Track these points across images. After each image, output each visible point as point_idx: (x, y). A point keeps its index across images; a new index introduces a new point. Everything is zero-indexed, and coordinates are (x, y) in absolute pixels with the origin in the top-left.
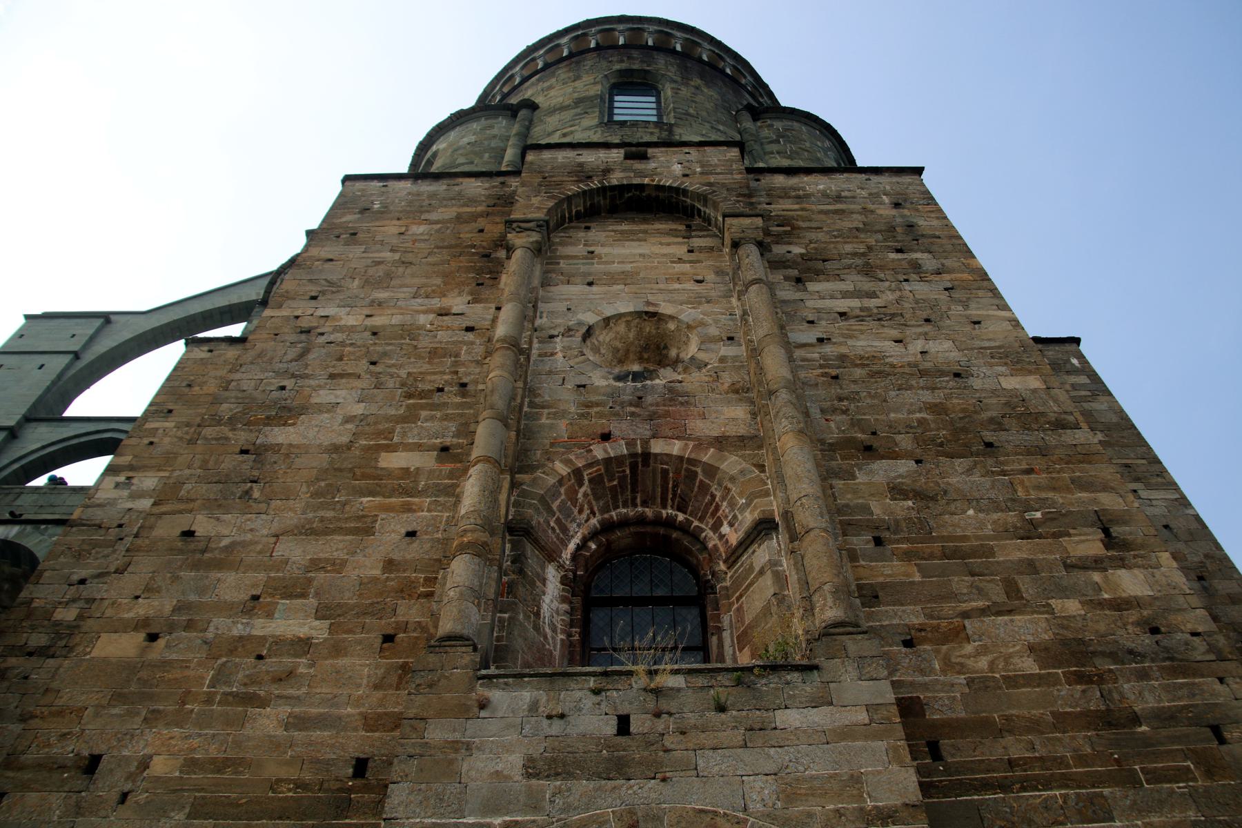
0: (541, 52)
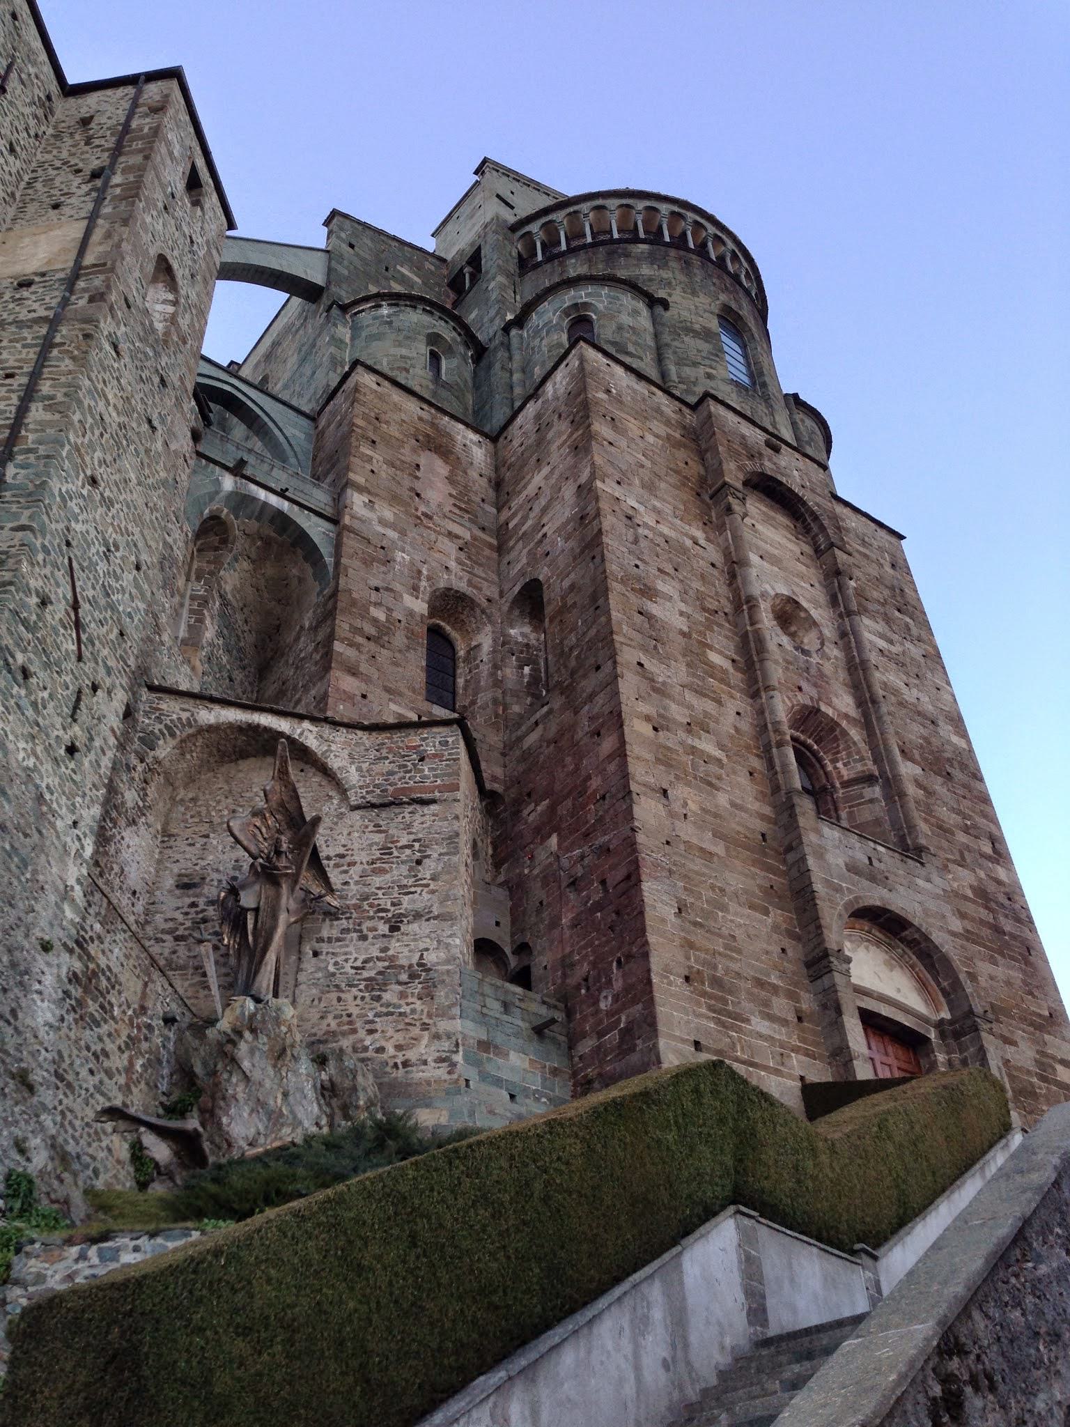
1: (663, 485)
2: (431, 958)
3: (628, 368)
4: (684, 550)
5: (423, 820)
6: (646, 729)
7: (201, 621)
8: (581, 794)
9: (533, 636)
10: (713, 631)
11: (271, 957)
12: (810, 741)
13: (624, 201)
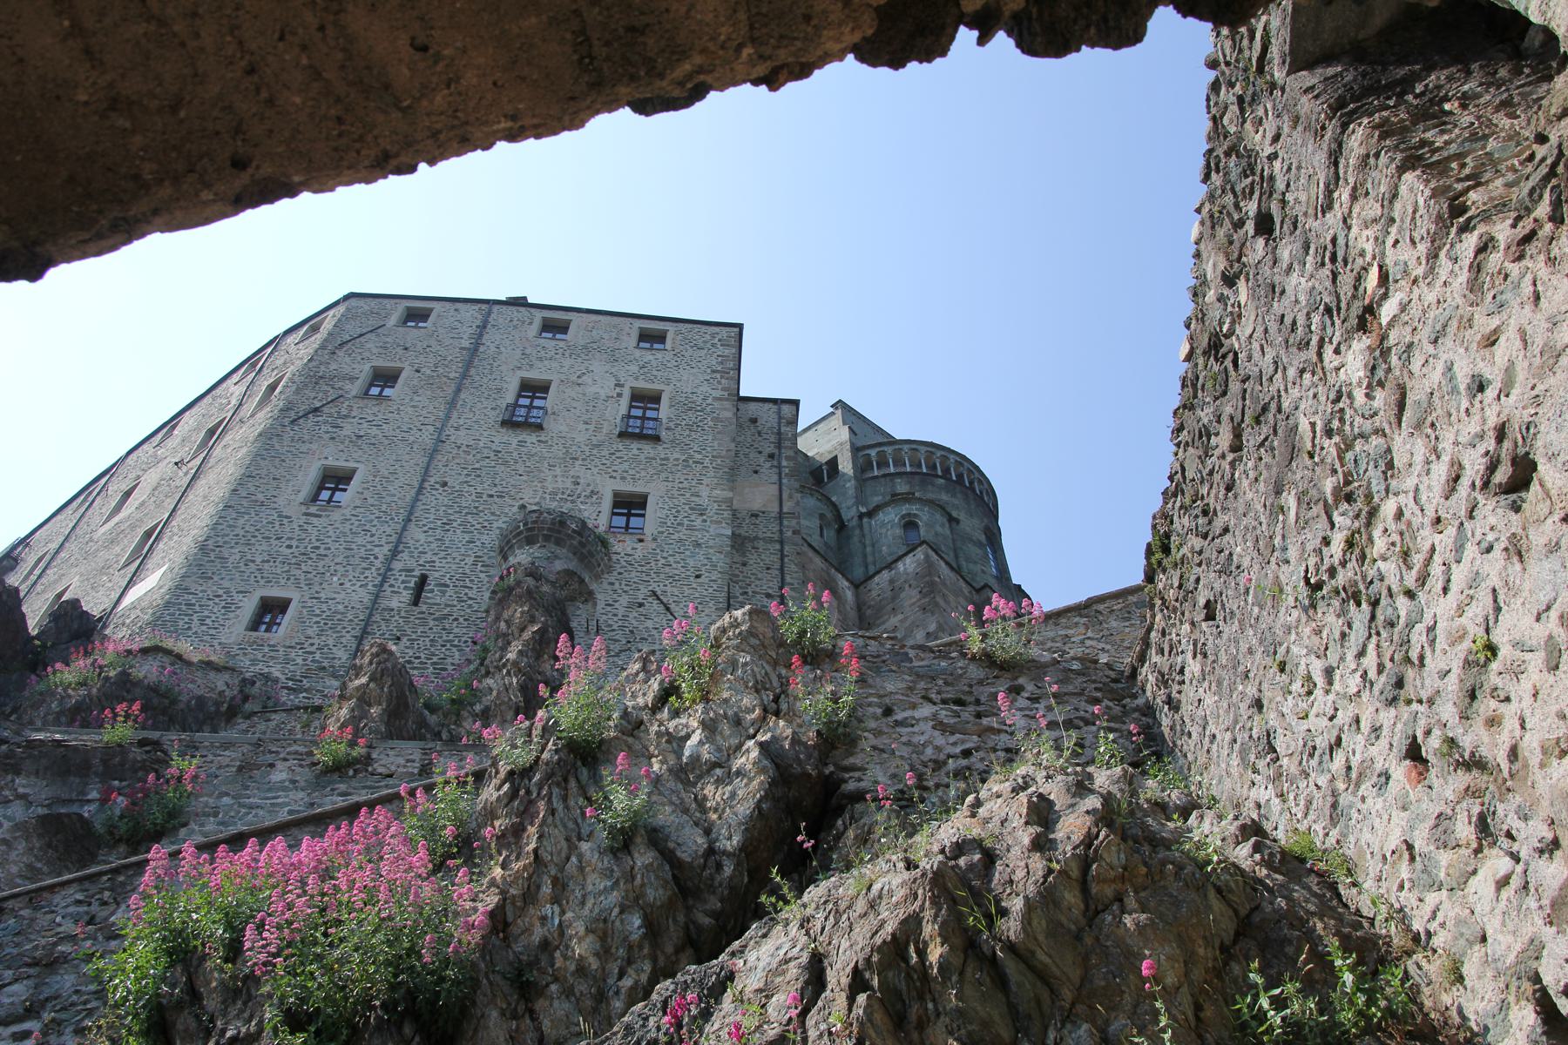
0: (939, 453)
3: (947, 563)
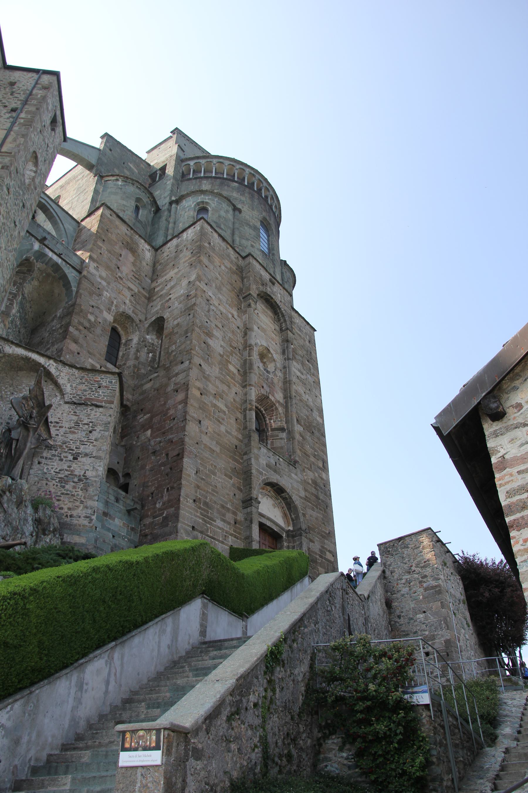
1: (224, 289)
2: (89, 474)
3: (220, 235)
4: (228, 319)
5: (96, 414)
6: (197, 393)
7: (12, 304)
8: (165, 415)
9: (156, 340)
10: (232, 356)
11: (21, 462)
12: (262, 409)
13: (232, 163)
